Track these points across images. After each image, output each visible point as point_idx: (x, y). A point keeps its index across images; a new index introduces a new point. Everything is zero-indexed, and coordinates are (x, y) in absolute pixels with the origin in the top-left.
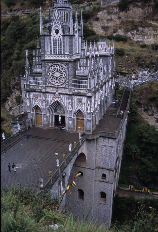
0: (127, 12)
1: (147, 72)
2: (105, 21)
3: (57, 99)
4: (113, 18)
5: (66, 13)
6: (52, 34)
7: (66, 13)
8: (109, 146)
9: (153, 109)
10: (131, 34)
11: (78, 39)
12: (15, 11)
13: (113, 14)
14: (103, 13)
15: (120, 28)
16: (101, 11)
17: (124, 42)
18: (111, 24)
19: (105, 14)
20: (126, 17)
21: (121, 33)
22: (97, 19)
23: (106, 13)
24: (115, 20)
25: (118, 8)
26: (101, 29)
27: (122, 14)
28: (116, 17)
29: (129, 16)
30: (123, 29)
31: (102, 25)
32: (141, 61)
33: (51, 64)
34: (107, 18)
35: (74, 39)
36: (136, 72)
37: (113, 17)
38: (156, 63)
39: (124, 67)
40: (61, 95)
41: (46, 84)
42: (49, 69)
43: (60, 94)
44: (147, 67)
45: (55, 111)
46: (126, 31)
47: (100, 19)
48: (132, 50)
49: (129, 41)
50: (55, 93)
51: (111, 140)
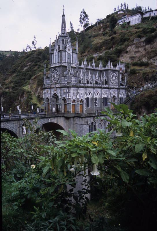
0: (152, 44)
1: (151, 85)
2: (133, 53)
3: (55, 92)
4: (140, 50)
5: (63, 39)
6: (55, 52)
7: (63, 39)
8: (80, 124)
9: (144, 111)
10: (153, 60)
11: (72, 55)
12: (84, 56)
13: (140, 47)
14: (132, 47)
15: (144, 57)
16: (130, 46)
17: (146, 67)
18: (137, 55)
19: (133, 48)
20: (151, 49)
21: (145, 60)
22: (127, 52)
23: (135, 47)
24: (142, 52)
25: (145, 43)
26: (129, 59)
27: (148, 47)
28: (143, 49)
29: (154, 47)
30: (147, 57)
31: (130, 56)
32: (146, 76)
33: (53, 70)
34: (135, 51)
35: (66, 53)
36: (143, 86)
37: (140, 49)
38: (155, 76)
39: (135, 83)
40: (57, 89)
41: (51, 83)
42: (52, 73)
43: (56, 88)
44: (150, 80)
45: (57, 101)
46: (149, 58)
47: (129, 52)
48: (141, 70)
49: (151, 66)
50: (54, 88)
51: (80, 118)
